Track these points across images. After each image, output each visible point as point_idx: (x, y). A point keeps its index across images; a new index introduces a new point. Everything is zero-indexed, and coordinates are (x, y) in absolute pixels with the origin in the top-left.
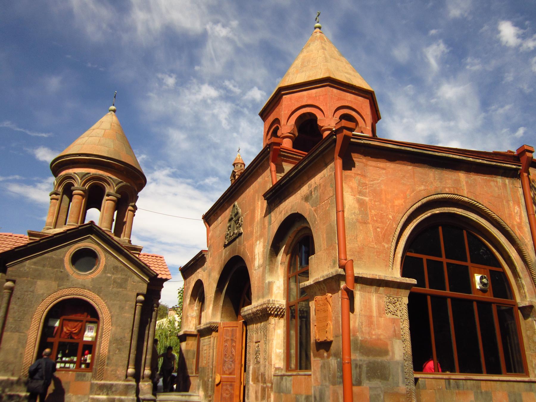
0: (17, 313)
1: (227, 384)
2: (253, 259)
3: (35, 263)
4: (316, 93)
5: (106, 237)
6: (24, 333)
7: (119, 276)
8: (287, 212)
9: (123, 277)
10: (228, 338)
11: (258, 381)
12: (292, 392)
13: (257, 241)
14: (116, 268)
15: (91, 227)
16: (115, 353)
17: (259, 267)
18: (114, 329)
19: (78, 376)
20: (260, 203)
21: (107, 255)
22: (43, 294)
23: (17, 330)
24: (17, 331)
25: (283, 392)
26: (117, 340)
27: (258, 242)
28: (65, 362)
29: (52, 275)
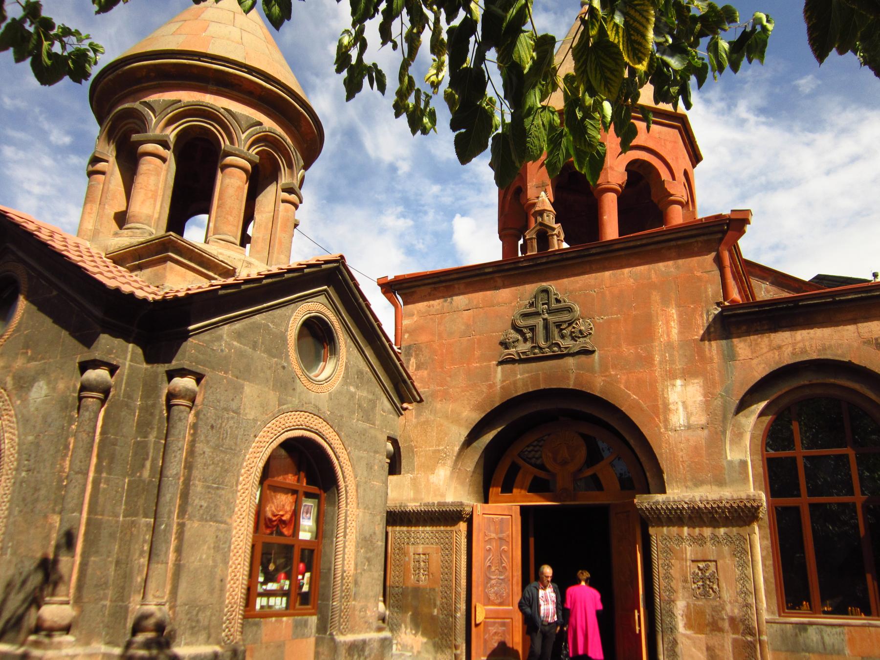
0: (211, 467)
1: (495, 623)
2: (662, 409)
3: (239, 336)
4: (660, 133)
5: (357, 300)
6: (225, 523)
7: (365, 394)
8: (804, 351)
9: (370, 397)
10: (493, 535)
11: (720, 630)
12: (847, 652)
13: (674, 378)
14: (360, 373)
15: (337, 268)
16: (364, 570)
17: (689, 427)
18: (361, 514)
19: (297, 625)
20: (673, 312)
21: (349, 340)
22: (255, 420)
23: (212, 515)
24: (214, 518)
25: (808, 649)
26: (365, 539)
27: (679, 382)
28: (269, 594)
29: (268, 372)
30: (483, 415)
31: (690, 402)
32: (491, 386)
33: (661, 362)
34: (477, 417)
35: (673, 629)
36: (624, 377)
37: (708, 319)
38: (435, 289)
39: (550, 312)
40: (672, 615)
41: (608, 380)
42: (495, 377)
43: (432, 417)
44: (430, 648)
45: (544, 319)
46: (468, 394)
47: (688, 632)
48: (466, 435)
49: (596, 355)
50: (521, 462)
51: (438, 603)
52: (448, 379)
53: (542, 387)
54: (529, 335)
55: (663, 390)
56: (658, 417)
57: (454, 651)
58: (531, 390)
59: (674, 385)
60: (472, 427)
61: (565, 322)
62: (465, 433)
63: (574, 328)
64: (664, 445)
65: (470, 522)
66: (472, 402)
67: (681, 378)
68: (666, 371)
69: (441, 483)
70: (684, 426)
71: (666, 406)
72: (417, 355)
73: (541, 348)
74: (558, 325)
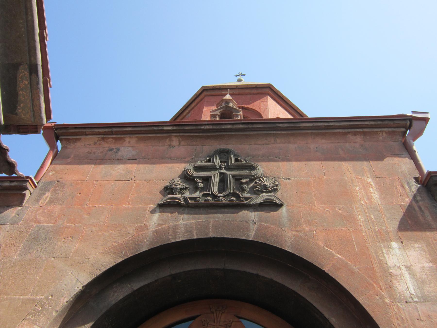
30: (120, 260)
31: (417, 267)
37: (411, 190)
38: (103, 139)
39: (228, 168)
41: (302, 235)
45: (221, 174)
46: (107, 234)
49: (283, 210)
52: (86, 216)
53: (211, 235)
54: (200, 185)
60: (99, 273)
61: (246, 177)
63: (256, 183)
68: (375, 232)
70: (417, 297)
71: (385, 268)
72: (55, 191)
73: (214, 197)
74: (238, 179)
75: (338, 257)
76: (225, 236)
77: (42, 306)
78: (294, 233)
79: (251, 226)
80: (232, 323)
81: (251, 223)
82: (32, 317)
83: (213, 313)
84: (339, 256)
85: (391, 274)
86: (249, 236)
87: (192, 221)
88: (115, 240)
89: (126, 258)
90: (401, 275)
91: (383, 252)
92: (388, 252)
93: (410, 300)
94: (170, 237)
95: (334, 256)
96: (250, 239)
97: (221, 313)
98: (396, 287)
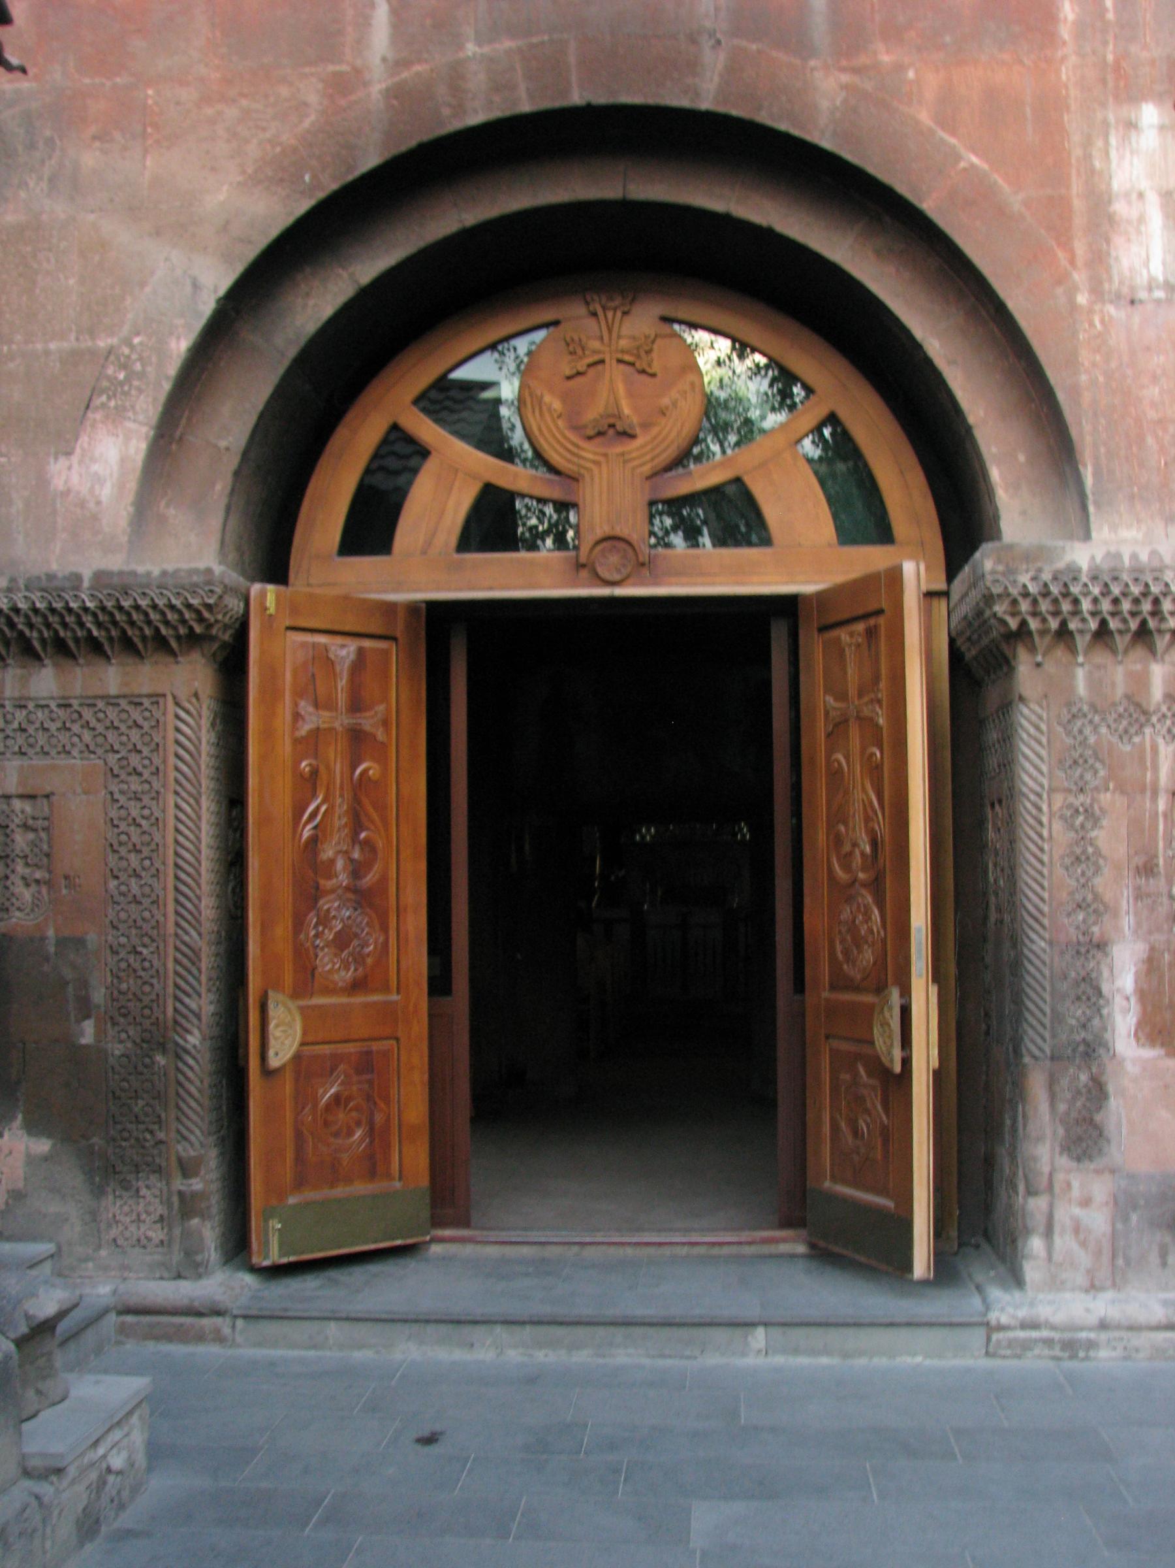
30: (303, 206)
32: (341, 85)
33: (1081, 30)
34: (272, 213)
35: (1091, 1049)
36: (932, 82)
40: (1090, 992)
41: (868, 86)
42: (361, 42)
43: (59, 209)
44: (73, 1178)
46: (232, 113)
47: (1149, 1053)
48: (222, 291)
50: (426, 429)
51: (99, 996)
53: (576, 98)
55: (1088, 143)
56: (1066, 243)
57: (178, 1184)
58: (526, 107)
59: (1131, 126)
60: (251, 253)
62: (217, 279)
64: (1085, 357)
65: (232, 665)
66: (253, 150)
67: (1158, 98)
69: (106, 492)
75: (972, 165)
76: (625, 99)
77: (124, 367)
78: (845, 78)
79: (708, 55)
80: (653, 342)
81: (706, 44)
82: (109, 398)
83: (595, 314)
84: (975, 160)
85: (1111, 219)
86: (697, 95)
87: (508, 44)
88: (268, 135)
89: (321, 195)
90: (1142, 219)
91: (1107, 143)
92: (1125, 139)
93: (1143, 295)
94: (446, 112)
95: (958, 158)
96: (705, 105)
97: (619, 314)
98: (1117, 258)
